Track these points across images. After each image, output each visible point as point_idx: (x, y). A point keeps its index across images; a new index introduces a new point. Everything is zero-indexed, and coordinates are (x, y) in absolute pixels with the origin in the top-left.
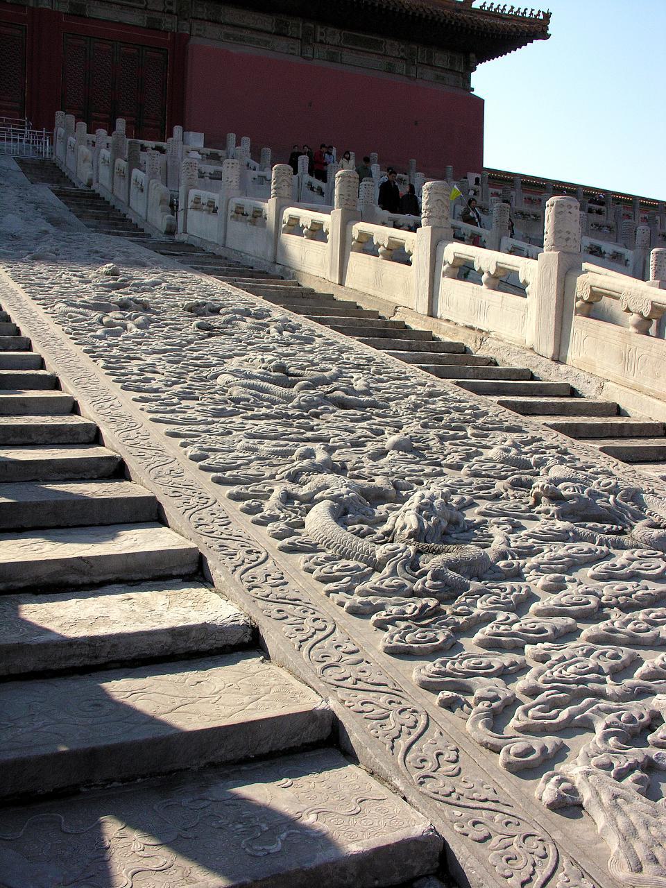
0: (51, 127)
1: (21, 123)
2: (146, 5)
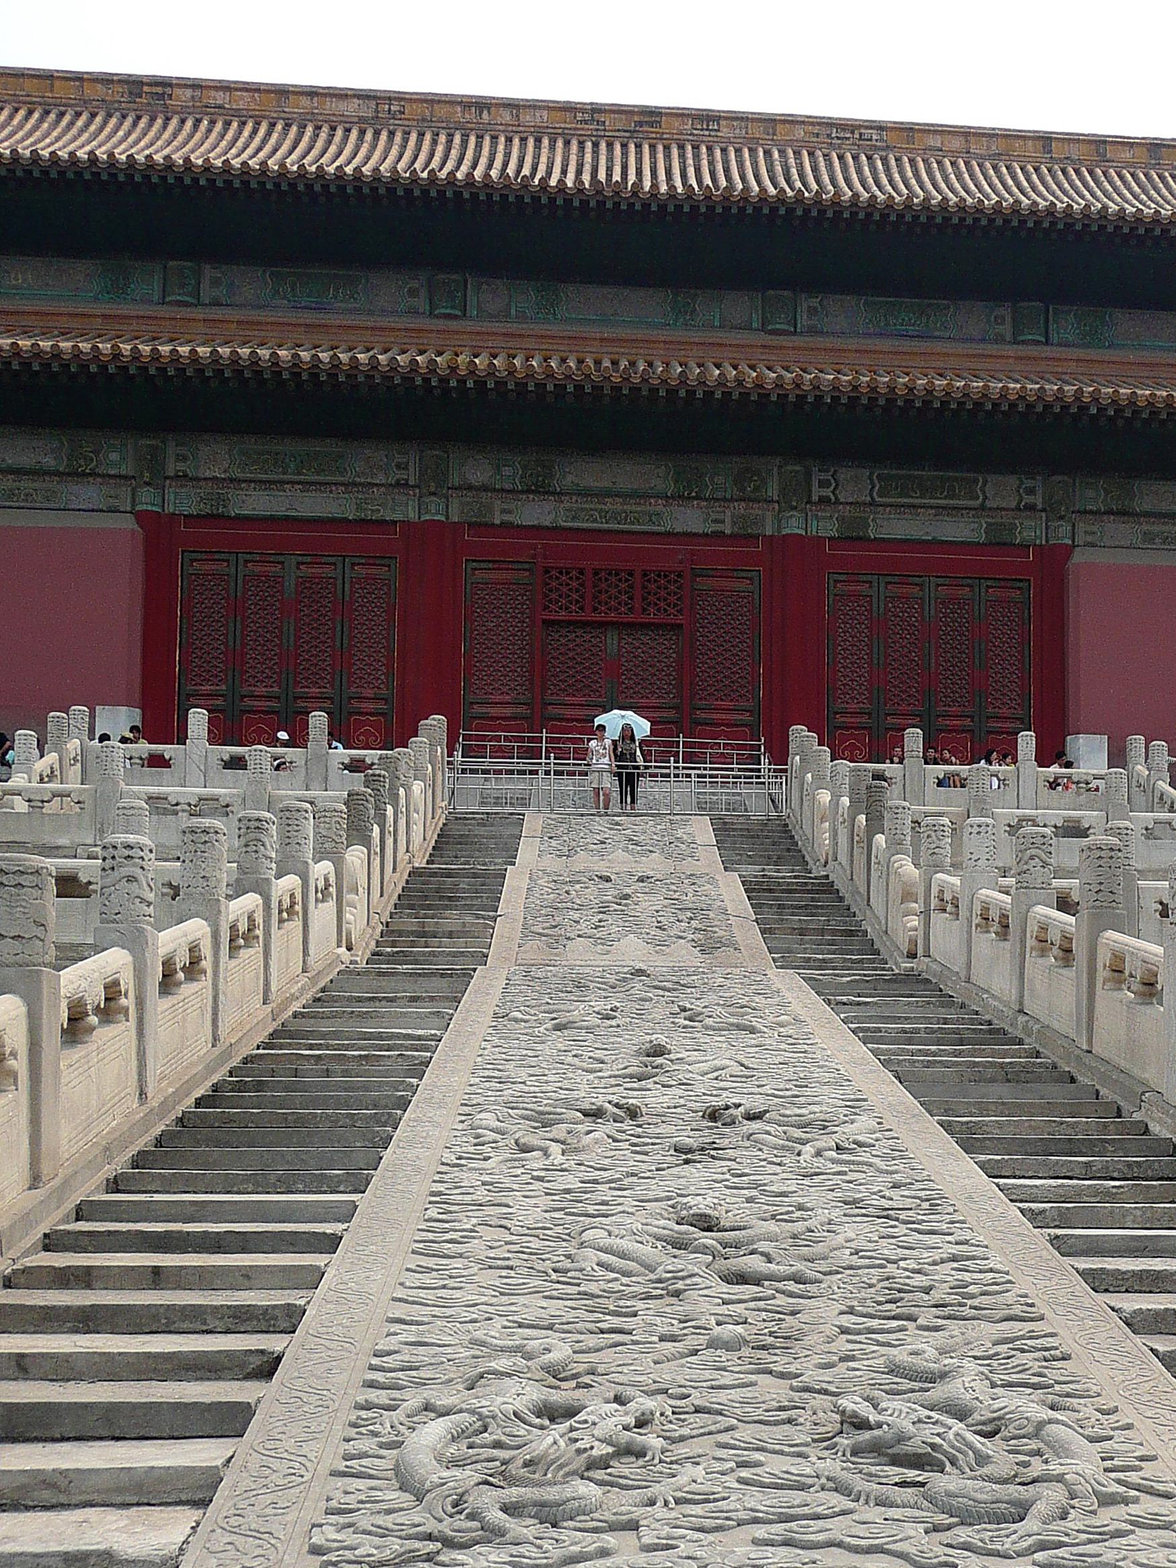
0: (780, 755)
1: (752, 748)
2: (984, 500)
